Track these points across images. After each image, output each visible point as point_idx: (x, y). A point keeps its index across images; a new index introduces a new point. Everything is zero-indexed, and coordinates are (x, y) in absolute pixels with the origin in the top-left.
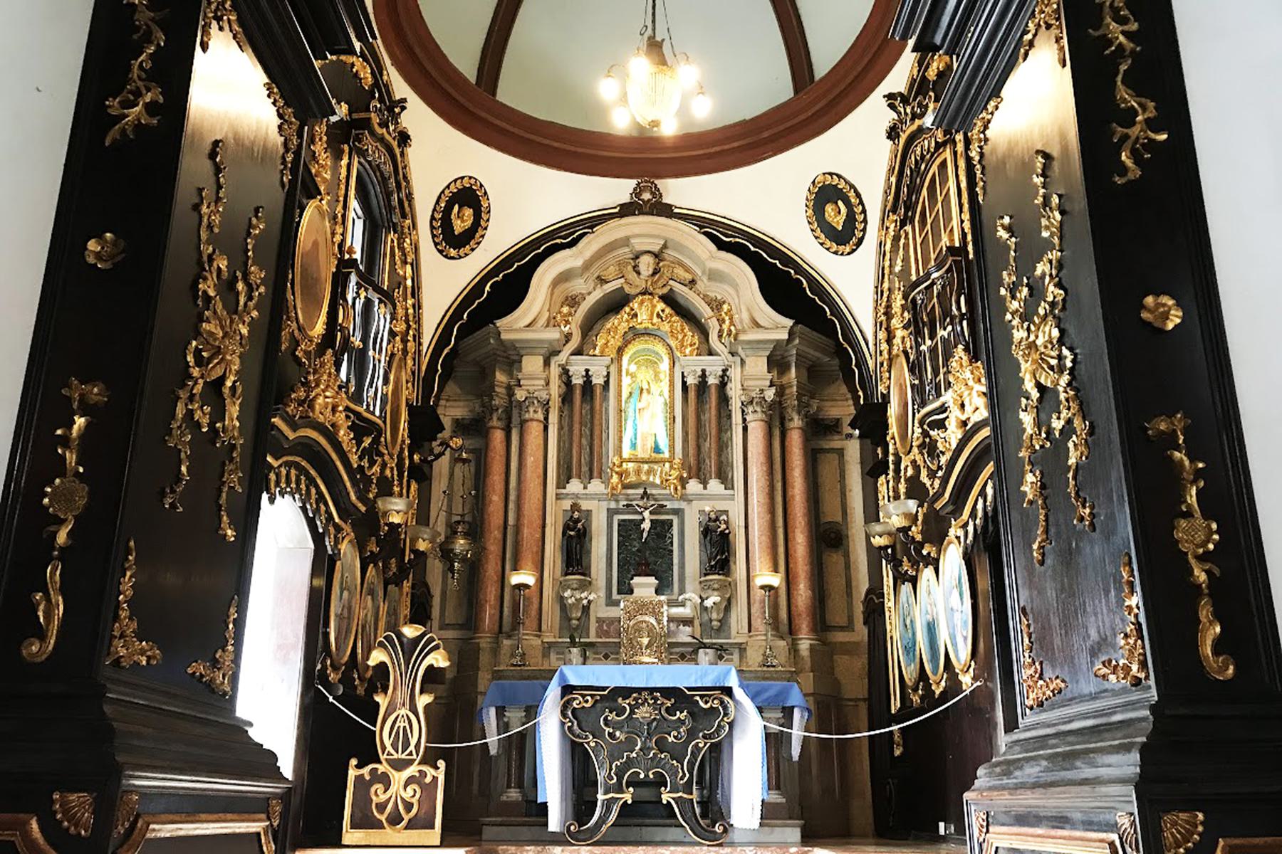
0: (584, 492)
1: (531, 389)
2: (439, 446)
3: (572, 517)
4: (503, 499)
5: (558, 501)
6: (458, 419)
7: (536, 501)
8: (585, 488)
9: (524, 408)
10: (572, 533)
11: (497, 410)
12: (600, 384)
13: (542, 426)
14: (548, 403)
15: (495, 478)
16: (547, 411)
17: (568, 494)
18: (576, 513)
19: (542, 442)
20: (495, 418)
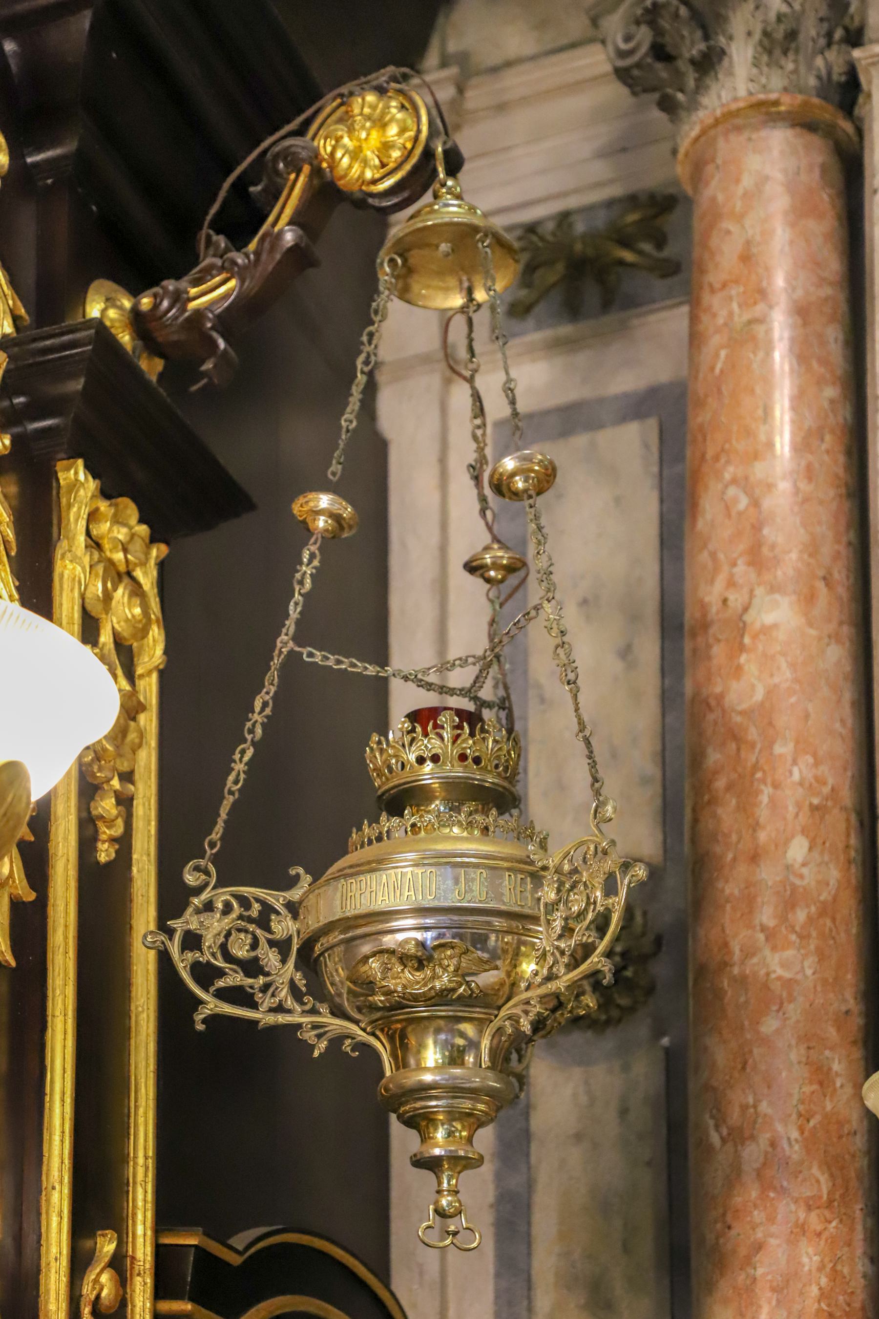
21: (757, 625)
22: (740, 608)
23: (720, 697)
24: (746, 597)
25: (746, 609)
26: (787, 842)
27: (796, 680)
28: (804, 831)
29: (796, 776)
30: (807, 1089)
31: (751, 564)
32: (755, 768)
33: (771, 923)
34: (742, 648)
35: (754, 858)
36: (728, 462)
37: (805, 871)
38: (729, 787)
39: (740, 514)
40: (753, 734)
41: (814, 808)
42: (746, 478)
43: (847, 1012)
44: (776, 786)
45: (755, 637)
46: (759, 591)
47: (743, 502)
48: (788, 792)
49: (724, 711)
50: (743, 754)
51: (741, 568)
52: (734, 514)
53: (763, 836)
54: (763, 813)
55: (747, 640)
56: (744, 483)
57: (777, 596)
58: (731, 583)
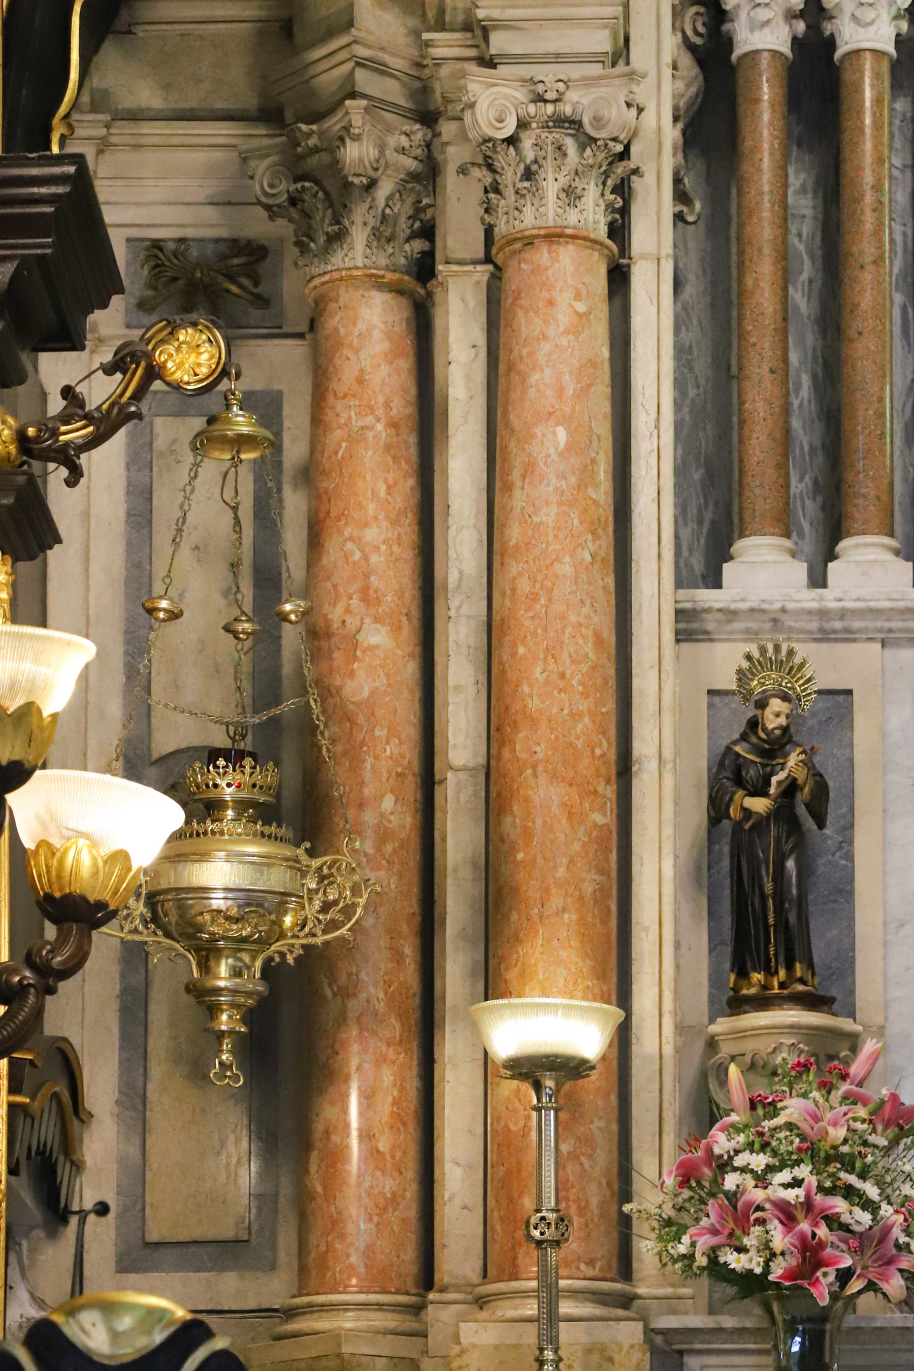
0: (810, 599)
1: (548, 74)
2: (109, 370)
3: (754, 724)
4: (409, 632)
5: (685, 646)
6: (157, 245)
7: (589, 649)
8: (818, 580)
9: (510, 176)
10: (759, 805)
11: (372, 185)
12: (877, 53)
13: (602, 270)
14: (625, 154)
15: (371, 535)
16: (623, 189)
17: (731, 614)
18: (776, 704)
19: (606, 353)
20: (359, 236)
21: (365, 644)
22: (354, 630)
23: (339, 689)
24: (359, 623)
25: (358, 632)
26: (382, 796)
27: (389, 685)
28: (392, 791)
29: (388, 752)
30: (390, 965)
31: (362, 600)
32: (363, 743)
33: (371, 851)
34: (355, 658)
35: (361, 806)
36: (346, 524)
37: (392, 817)
38: (345, 753)
39: (354, 563)
40: (361, 719)
41: (399, 775)
42: (360, 539)
43: (414, 914)
44: (376, 758)
45: (364, 652)
46: (367, 620)
47: (357, 556)
48: (383, 763)
49: (341, 699)
50: (355, 733)
51: (355, 602)
52: (351, 560)
53: (367, 791)
54: (367, 775)
55: (358, 653)
56: (357, 540)
57: (378, 626)
58: (348, 610)
